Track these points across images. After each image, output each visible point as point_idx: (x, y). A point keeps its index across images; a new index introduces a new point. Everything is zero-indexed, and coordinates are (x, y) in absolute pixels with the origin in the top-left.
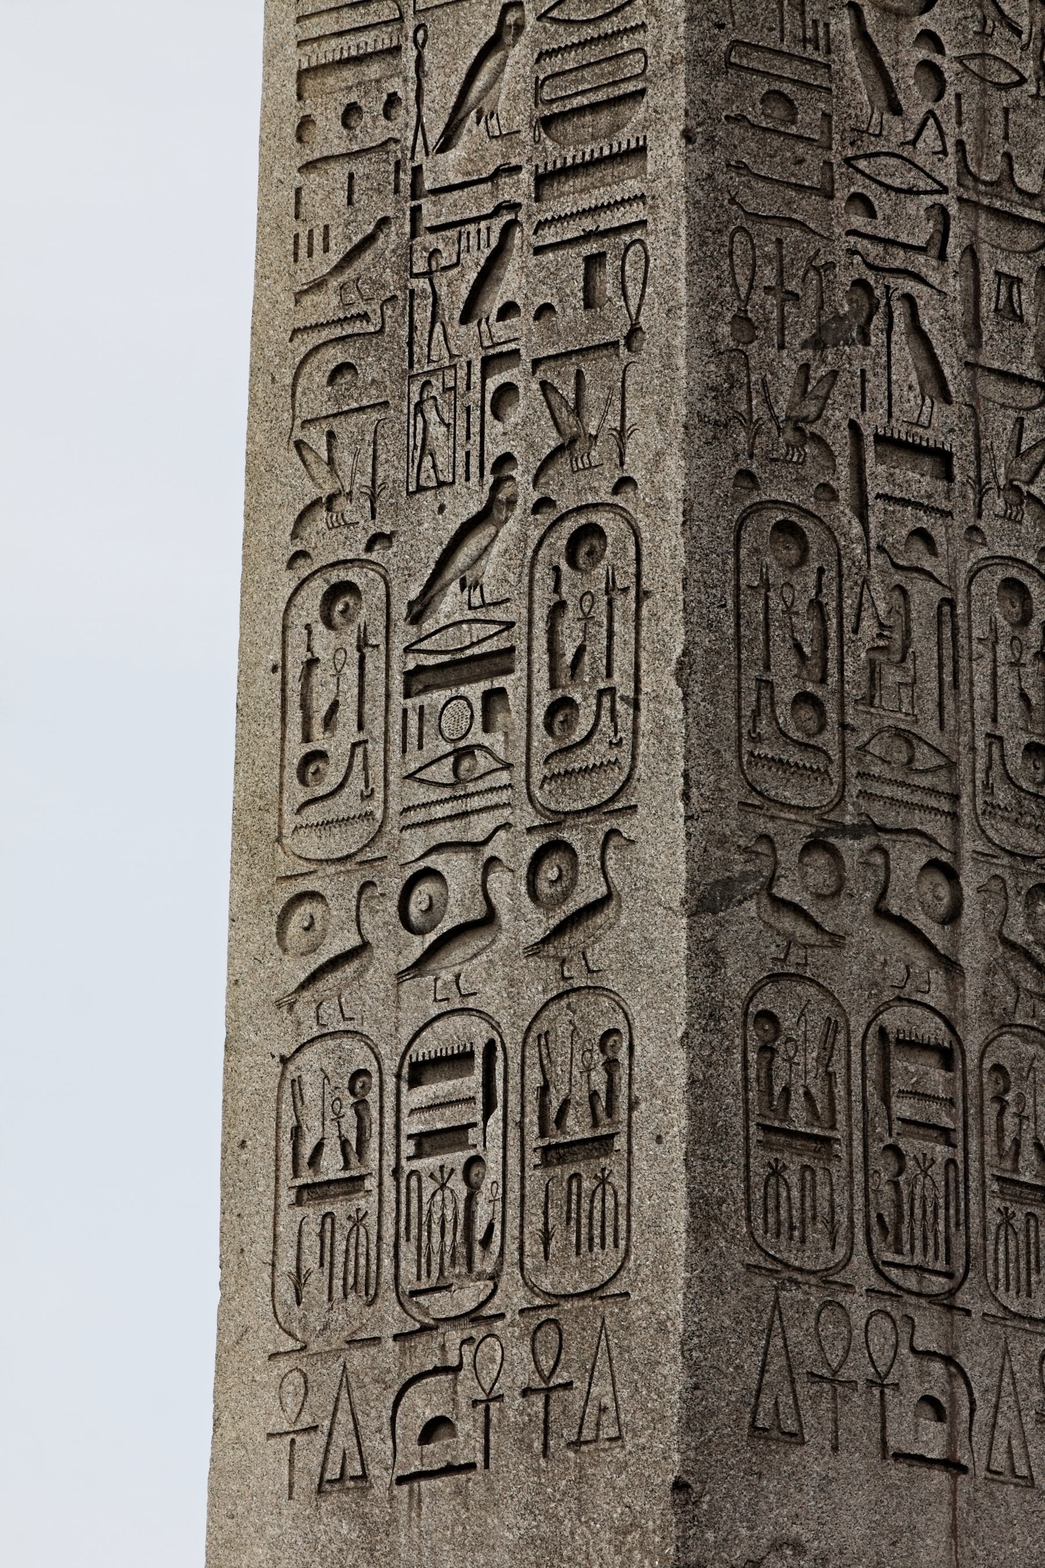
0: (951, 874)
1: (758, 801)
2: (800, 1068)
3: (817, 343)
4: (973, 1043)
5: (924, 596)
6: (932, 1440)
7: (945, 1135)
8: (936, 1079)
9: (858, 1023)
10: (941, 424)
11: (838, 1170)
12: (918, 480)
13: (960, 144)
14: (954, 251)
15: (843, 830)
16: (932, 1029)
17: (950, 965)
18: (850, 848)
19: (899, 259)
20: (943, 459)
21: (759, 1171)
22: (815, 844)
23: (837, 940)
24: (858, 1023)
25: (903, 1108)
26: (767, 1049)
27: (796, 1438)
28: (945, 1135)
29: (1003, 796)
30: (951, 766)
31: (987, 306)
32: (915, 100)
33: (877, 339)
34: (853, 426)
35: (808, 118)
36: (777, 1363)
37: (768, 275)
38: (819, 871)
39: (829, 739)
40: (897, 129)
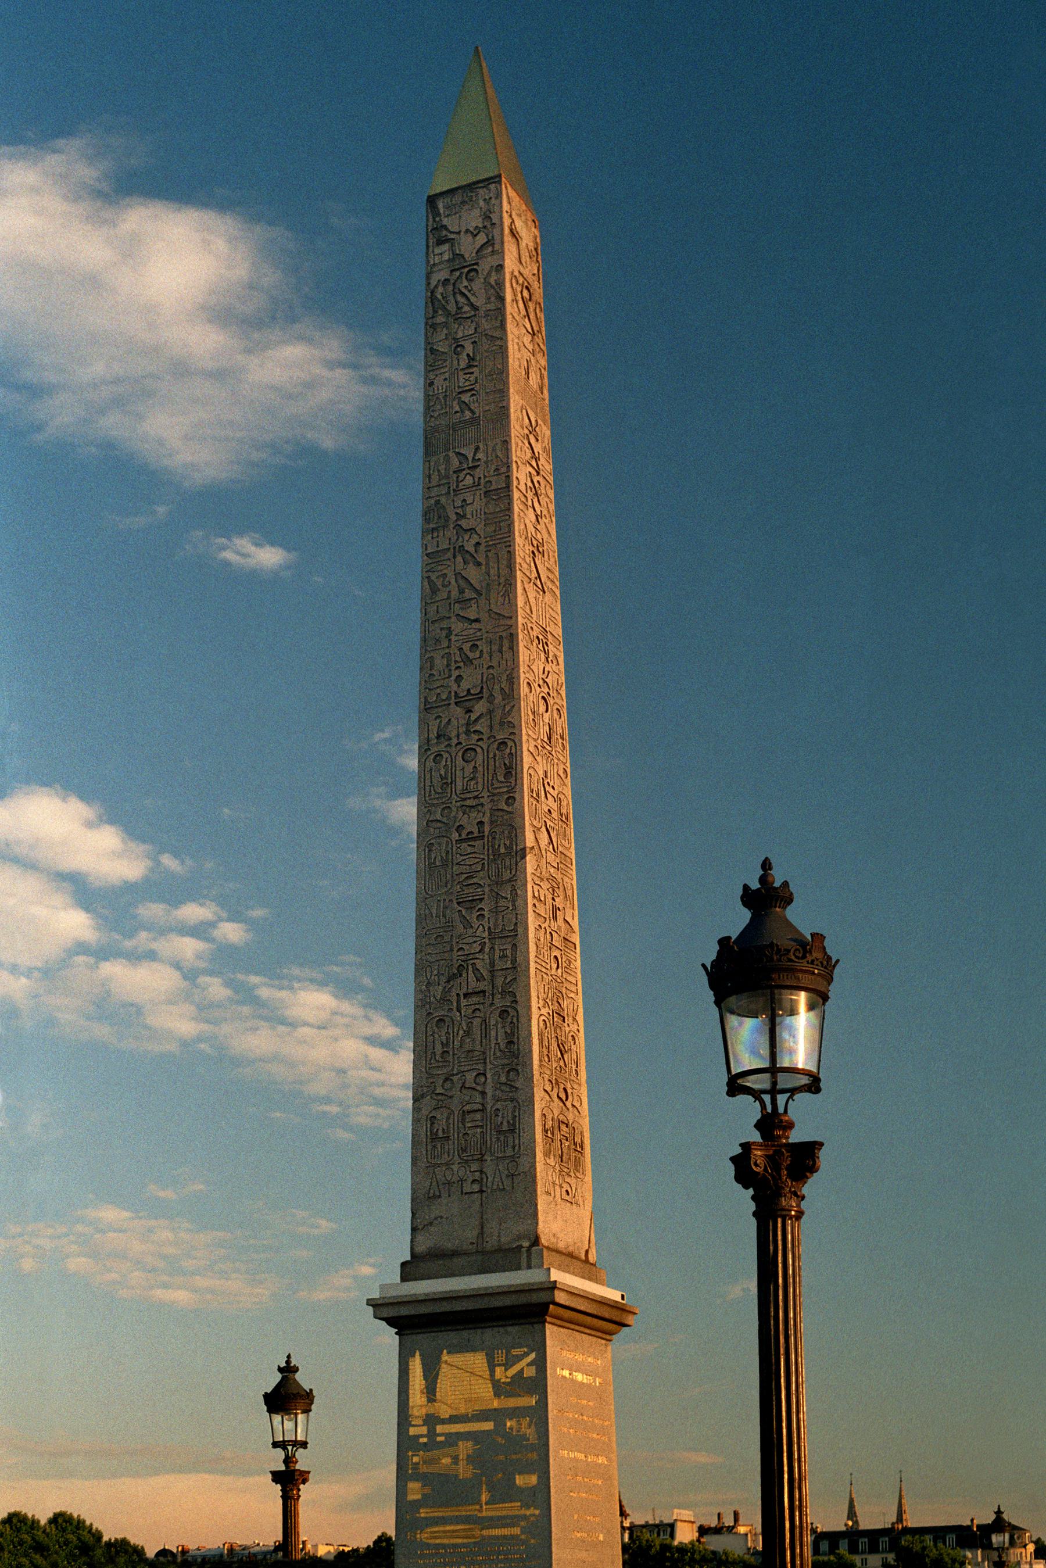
0: (484, 1075)
1: (430, 1075)
2: (441, 1125)
3: (448, 981)
4: (489, 1107)
5: (477, 1022)
6: (476, 1187)
7: (482, 1127)
8: (478, 1116)
9: (456, 1113)
10: (482, 986)
11: (450, 1142)
12: (475, 999)
13: (489, 928)
14: (487, 950)
15: (453, 1075)
16: (480, 1107)
17: (483, 1093)
18: (455, 1078)
19: (471, 957)
20: (484, 992)
21: (429, 1147)
22: (446, 1079)
23: (451, 1097)
24: (456, 1113)
25: (469, 1125)
26: (432, 1124)
27: (440, 1196)
28: (482, 1127)
29: (498, 1054)
30: (484, 1053)
31: (497, 957)
32: (475, 923)
33: (464, 975)
34: (458, 995)
35: (447, 938)
36: (434, 1184)
37: (436, 972)
38: (448, 1085)
39: (450, 1059)
40: (470, 931)
